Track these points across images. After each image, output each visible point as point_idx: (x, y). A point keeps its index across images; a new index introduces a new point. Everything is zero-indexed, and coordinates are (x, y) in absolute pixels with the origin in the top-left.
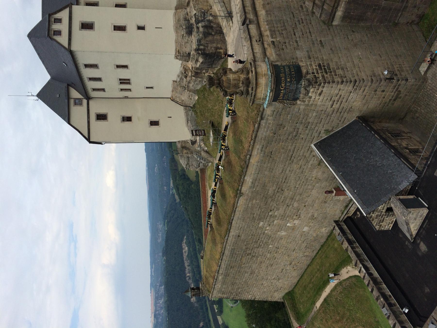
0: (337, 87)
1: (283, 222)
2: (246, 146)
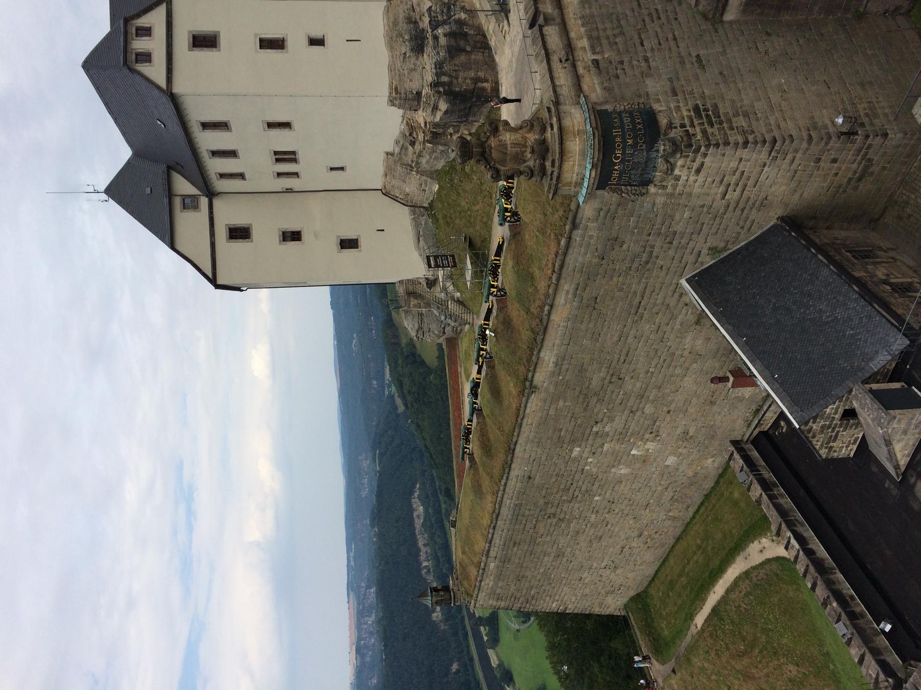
0: (735, 153)
1: (623, 446)
2: (542, 285)
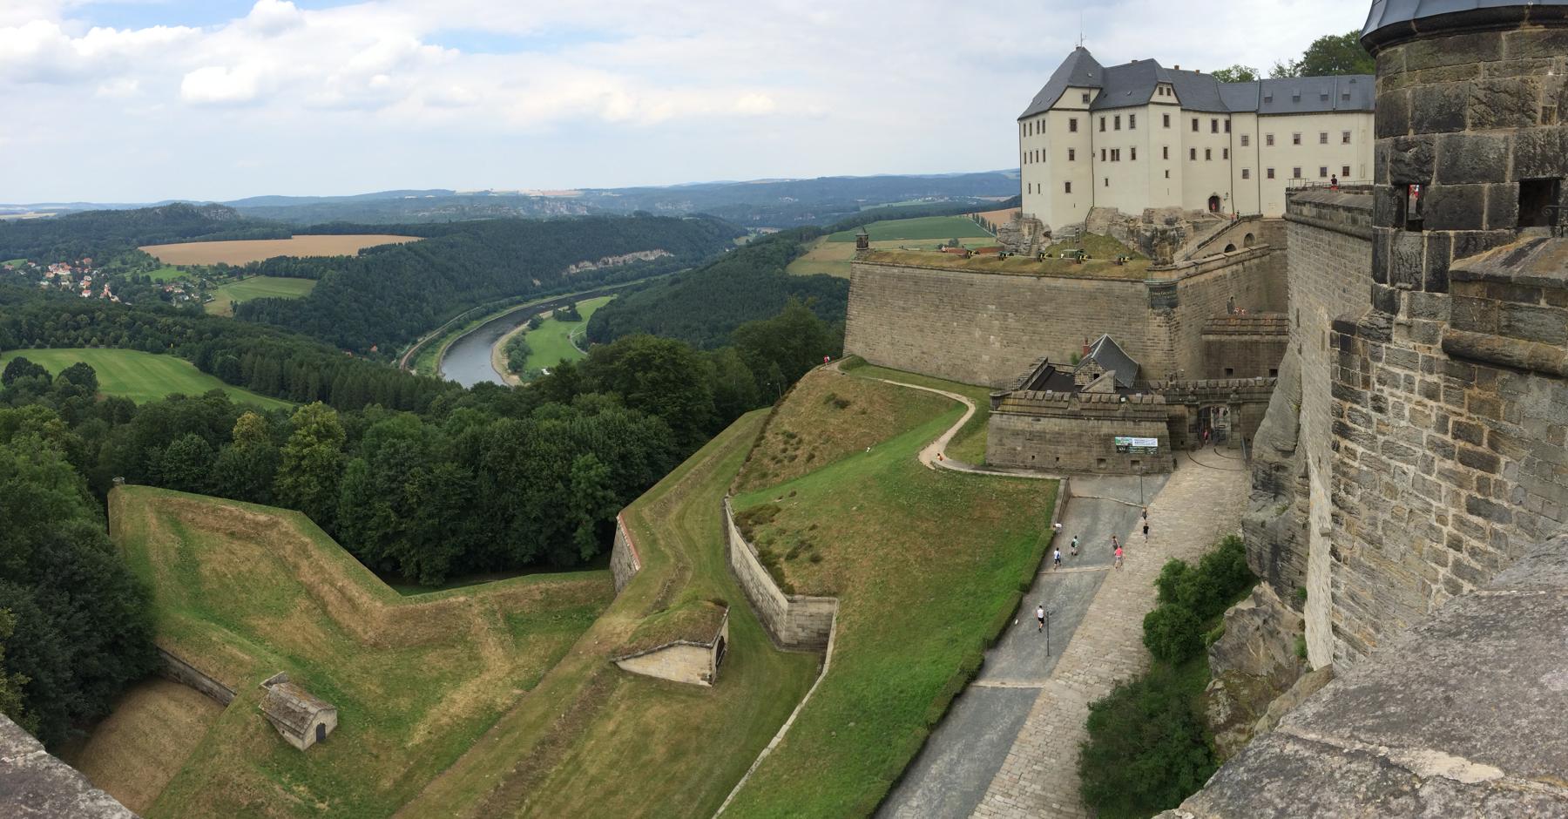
2: (1101, 274)
